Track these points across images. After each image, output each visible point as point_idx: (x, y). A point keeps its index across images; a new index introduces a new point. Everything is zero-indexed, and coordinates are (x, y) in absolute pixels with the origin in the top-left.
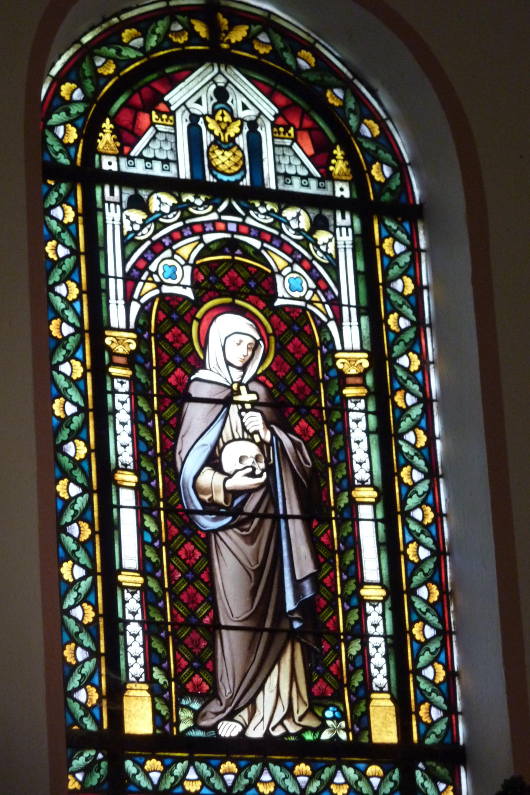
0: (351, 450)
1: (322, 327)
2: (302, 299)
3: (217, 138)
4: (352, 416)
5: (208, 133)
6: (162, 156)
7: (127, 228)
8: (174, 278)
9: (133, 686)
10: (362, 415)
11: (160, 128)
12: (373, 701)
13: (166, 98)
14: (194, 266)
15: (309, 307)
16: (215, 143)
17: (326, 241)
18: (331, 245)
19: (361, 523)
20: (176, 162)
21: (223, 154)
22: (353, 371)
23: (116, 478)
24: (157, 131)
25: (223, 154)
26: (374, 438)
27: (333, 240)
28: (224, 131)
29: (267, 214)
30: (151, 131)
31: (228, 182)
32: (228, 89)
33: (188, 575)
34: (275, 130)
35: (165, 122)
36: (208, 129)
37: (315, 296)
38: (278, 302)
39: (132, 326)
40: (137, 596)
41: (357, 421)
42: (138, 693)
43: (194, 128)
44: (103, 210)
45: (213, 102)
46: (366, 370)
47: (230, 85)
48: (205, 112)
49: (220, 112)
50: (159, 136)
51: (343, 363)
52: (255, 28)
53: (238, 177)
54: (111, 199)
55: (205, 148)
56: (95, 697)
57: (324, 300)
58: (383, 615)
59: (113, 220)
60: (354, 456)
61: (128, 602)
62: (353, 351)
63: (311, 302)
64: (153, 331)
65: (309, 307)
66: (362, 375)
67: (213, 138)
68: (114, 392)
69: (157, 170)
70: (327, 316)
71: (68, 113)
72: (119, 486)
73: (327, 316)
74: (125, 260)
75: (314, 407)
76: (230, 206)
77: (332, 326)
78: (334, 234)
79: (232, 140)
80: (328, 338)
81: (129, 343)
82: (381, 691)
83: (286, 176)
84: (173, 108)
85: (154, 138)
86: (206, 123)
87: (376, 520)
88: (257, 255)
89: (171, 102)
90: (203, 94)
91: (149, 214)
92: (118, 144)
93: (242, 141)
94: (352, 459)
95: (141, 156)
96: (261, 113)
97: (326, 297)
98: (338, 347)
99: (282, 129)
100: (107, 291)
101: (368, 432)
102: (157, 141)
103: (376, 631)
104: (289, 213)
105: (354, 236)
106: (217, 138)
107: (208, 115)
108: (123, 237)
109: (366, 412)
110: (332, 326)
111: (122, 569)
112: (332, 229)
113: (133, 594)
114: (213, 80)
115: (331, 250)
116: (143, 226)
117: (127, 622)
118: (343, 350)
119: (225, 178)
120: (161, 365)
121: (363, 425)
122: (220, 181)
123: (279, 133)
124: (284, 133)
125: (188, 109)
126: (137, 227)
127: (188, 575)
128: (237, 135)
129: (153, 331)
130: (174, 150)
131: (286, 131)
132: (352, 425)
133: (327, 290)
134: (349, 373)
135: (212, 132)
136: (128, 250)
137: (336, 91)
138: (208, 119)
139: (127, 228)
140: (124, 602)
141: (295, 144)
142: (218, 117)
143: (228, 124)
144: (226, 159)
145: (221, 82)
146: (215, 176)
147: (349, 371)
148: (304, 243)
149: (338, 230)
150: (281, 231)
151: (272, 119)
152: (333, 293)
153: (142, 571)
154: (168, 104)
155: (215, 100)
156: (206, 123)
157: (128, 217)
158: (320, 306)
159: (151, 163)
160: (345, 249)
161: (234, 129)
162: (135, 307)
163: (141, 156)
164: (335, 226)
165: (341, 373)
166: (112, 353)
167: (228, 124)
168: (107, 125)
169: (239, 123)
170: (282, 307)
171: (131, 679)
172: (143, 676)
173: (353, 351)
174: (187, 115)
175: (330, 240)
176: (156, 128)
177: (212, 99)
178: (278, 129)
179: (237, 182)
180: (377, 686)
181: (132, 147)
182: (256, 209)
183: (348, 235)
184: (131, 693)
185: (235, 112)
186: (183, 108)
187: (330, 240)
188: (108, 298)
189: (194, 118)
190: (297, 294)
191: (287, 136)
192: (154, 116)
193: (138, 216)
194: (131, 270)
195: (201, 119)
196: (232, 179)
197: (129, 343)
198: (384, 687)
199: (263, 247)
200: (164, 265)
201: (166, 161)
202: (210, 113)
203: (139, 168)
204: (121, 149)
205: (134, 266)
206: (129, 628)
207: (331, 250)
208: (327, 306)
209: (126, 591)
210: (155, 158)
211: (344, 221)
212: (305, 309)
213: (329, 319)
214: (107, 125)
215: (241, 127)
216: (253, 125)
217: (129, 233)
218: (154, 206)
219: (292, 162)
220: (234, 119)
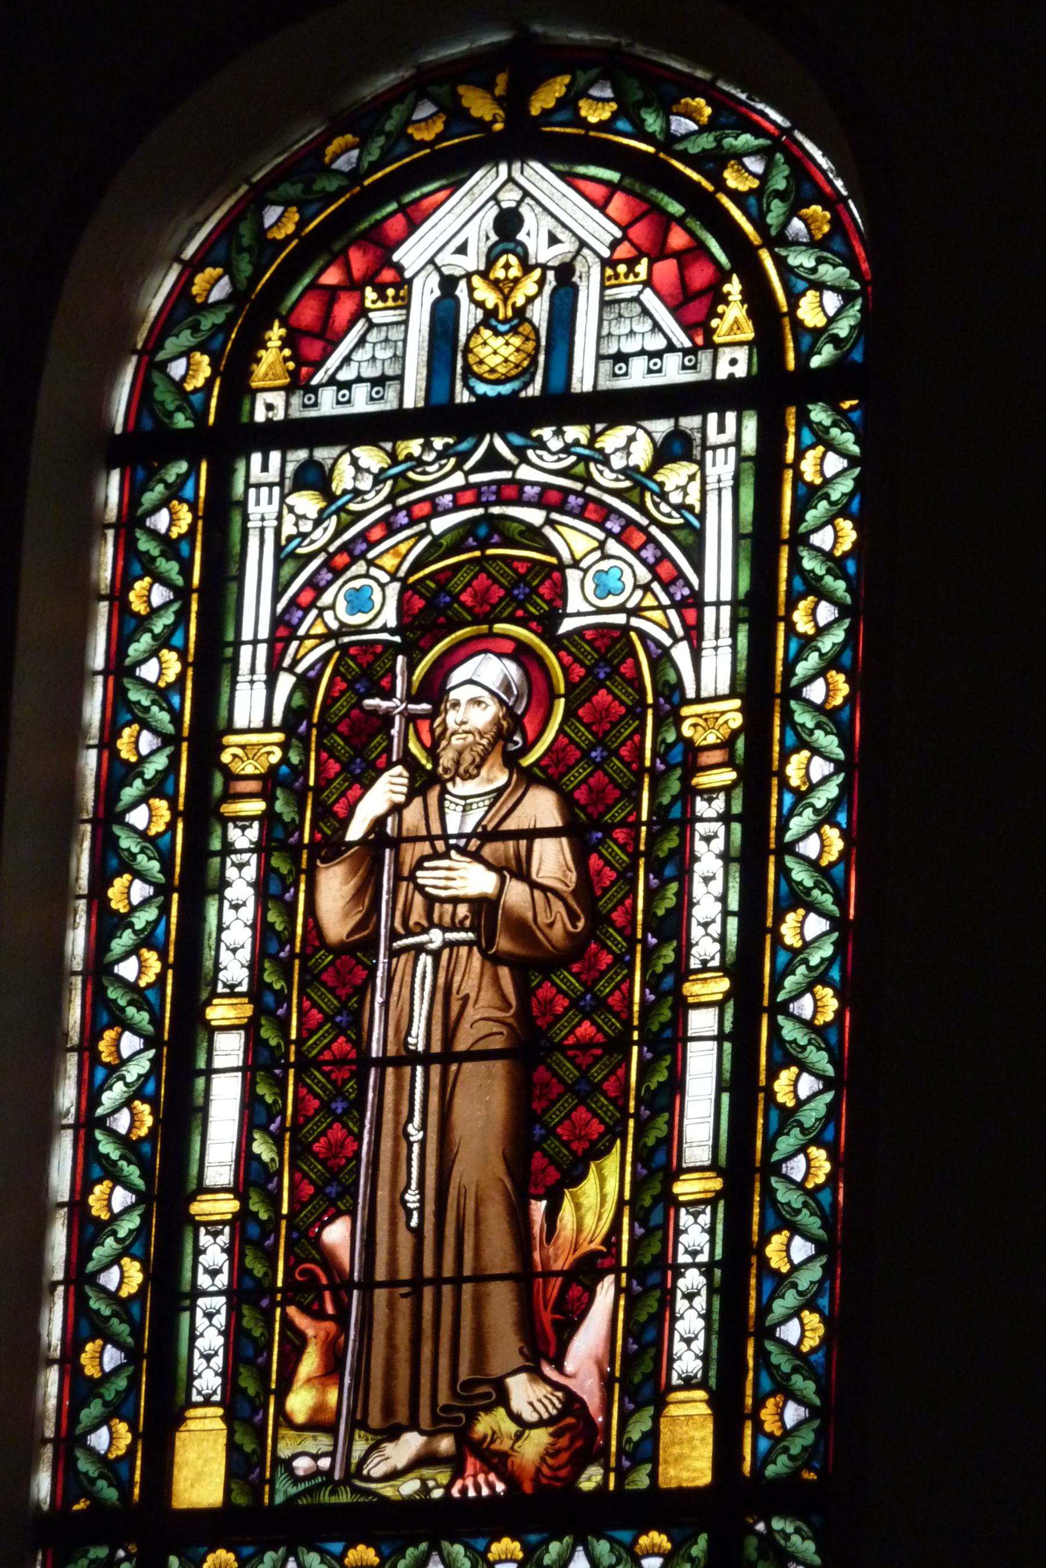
0: (690, 897)
1: (661, 658)
2: (620, 609)
3: (490, 314)
4: (701, 828)
5: (473, 306)
6: (369, 372)
7: (288, 528)
8: (598, 592)
9: (200, 1412)
10: (719, 828)
11: (376, 317)
12: (189, 1422)
13: (396, 257)
14: (403, 580)
15: (635, 622)
16: (485, 323)
17: (683, 481)
18: (694, 488)
19: (692, 1046)
20: (400, 378)
21: (507, 344)
22: (712, 739)
23: (208, 1017)
24: (371, 325)
25: (507, 344)
26: (735, 868)
27: (698, 476)
28: (506, 298)
29: (567, 450)
30: (360, 326)
31: (499, 395)
32: (524, 210)
33: (328, 1190)
34: (609, 272)
35: (622, 280)
36: (472, 300)
37: (649, 595)
38: (567, 625)
39: (277, 719)
40: (224, 1239)
41: (707, 839)
42: (209, 1424)
43: (448, 302)
44: (243, 504)
45: (490, 243)
46: (735, 734)
47: (528, 200)
48: (472, 268)
49: (502, 260)
50: (373, 336)
51: (695, 725)
52: (582, 78)
53: (514, 385)
54: (266, 478)
55: (462, 338)
56: (767, 1414)
57: (665, 601)
58: (711, 1231)
59: (263, 519)
60: (695, 911)
61: (685, 1231)
62: (249, 731)
63: (637, 611)
64: (315, 720)
65: (635, 622)
66: (727, 744)
67: (480, 314)
68: (228, 849)
69: (361, 402)
70: (670, 632)
71: (195, 328)
72: (212, 1030)
73: (670, 632)
74: (276, 597)
75: (623, 823)
76: (491, 448)
77: (681, 653)
78: (702, 464)
79: (520, 313)
80: (672, 678)
81: (269, 753)
82: (207, 1402)
83: (621, 358)
84: (408, 275)
85: (362, 342)
86: (471, 289)
87: (720, 1038)
88: (533, 536)
89: (405, 263)
90: (471, 233)
91: (330, 497)
92: (291, 365)
93: (539, 313)
94: (690, 916)
95: (332, 381)
96: (583, 244)
97: (671, 596)
98: (691, 693)
99: (622, 269)
100: (235, 660)
101: (725, 857)
102: (367, 345)
103: (213, 1285)
104: (613, 439)
105: (741, 459)
106: (490, 314)
107: (477, 272)
108: (278, 548)
109: (725, 818)
110: (681, 653)
111: (203, 1190)
112: (697, 452)
113: (696, 1215)
114: (494, 197)
115: (693, 498)
116: (318, 523)
117: (678, 1271)
118: (699, 700)
119: (491, 391)
120: (323, 783)
121: (718, 845)
122: (483, 398)
123: (617, 276)
124: (626, 276)
125: (438, 269)
126: (306, 527)
127: (328, 1190)
128: (530, 300)
129: (315, 720)
130: (400, 358)
131: (631, 270)
132: (700, 846)
133: (672, 580)
134: (704, 743)
135: (480, 304)
136: (287, 570)
137: (268, 221)
138: (476, 280)
139: (288, 528)
140: (198, 1251)
141: (648, 291)
142: (499, 273)
143: (516, 281)
144: (511, 349)
145: (510, 198)
146: (472, 391)
147: (705, 739)
148: (635, 496)
149: (709, 454)
150: (589, 480)
151: (606, 253)
152: (688, 584)
153: (239, 1190)
154: (399, 268)
155: (494, 238)
156: (471, 289)
157: (291, 509)
158: (657, 615)
159: (661, 360)
160: (720, 490)
161: (529, 287)
162: (286, 682)
163: (332, 381)
164: (705, 447)
165: (689, 742)
166: (230, 777)
167: (516, 281)
168: (276, 333)
169: (537, 273)
170: (579, 631)
171: (196, 1398)
172: (219, 1391)
173: (249, 731)
174: (435, 279)
175: (692, 478)
176: (369, 320)
177: (488, 238)
178: (614, 268)
179: (515, 393)
180: (199, 1393)
181: (318, 365)
182: (540, 444)
183: (270, 502)
184: (191, 1425)
185: (532, 251)
186: (430, 268)
187: (692, 478)
188: (235, 672)
189: (448, 283)
190: (612, 601)
191: (631, 278)
192: (370, 294)
193: (307, 503)
194: (287, 610)
195: (463, 285)
196: (506, 389)
197: (269, 753)
198: (214, 1392)
199: (427, 531)
200: (370, 586)
201: (380, 381)
202: (482, 267)
203: (328, 404)
204: (294, 374)
205: (293, 602)
206: (682, 1283)
207: (693, 498)
208: (672, 613)
209: (202, 1230)
210: (359, 380)
211: (265, 474)
212: (627, 628)
213: (676, 640)
214: (276, 333)
215: (541, 282)
216: (565, 272)
217: (290, 539)
218: (343, 479)
219: (377, 355)
220: (527, 268)
